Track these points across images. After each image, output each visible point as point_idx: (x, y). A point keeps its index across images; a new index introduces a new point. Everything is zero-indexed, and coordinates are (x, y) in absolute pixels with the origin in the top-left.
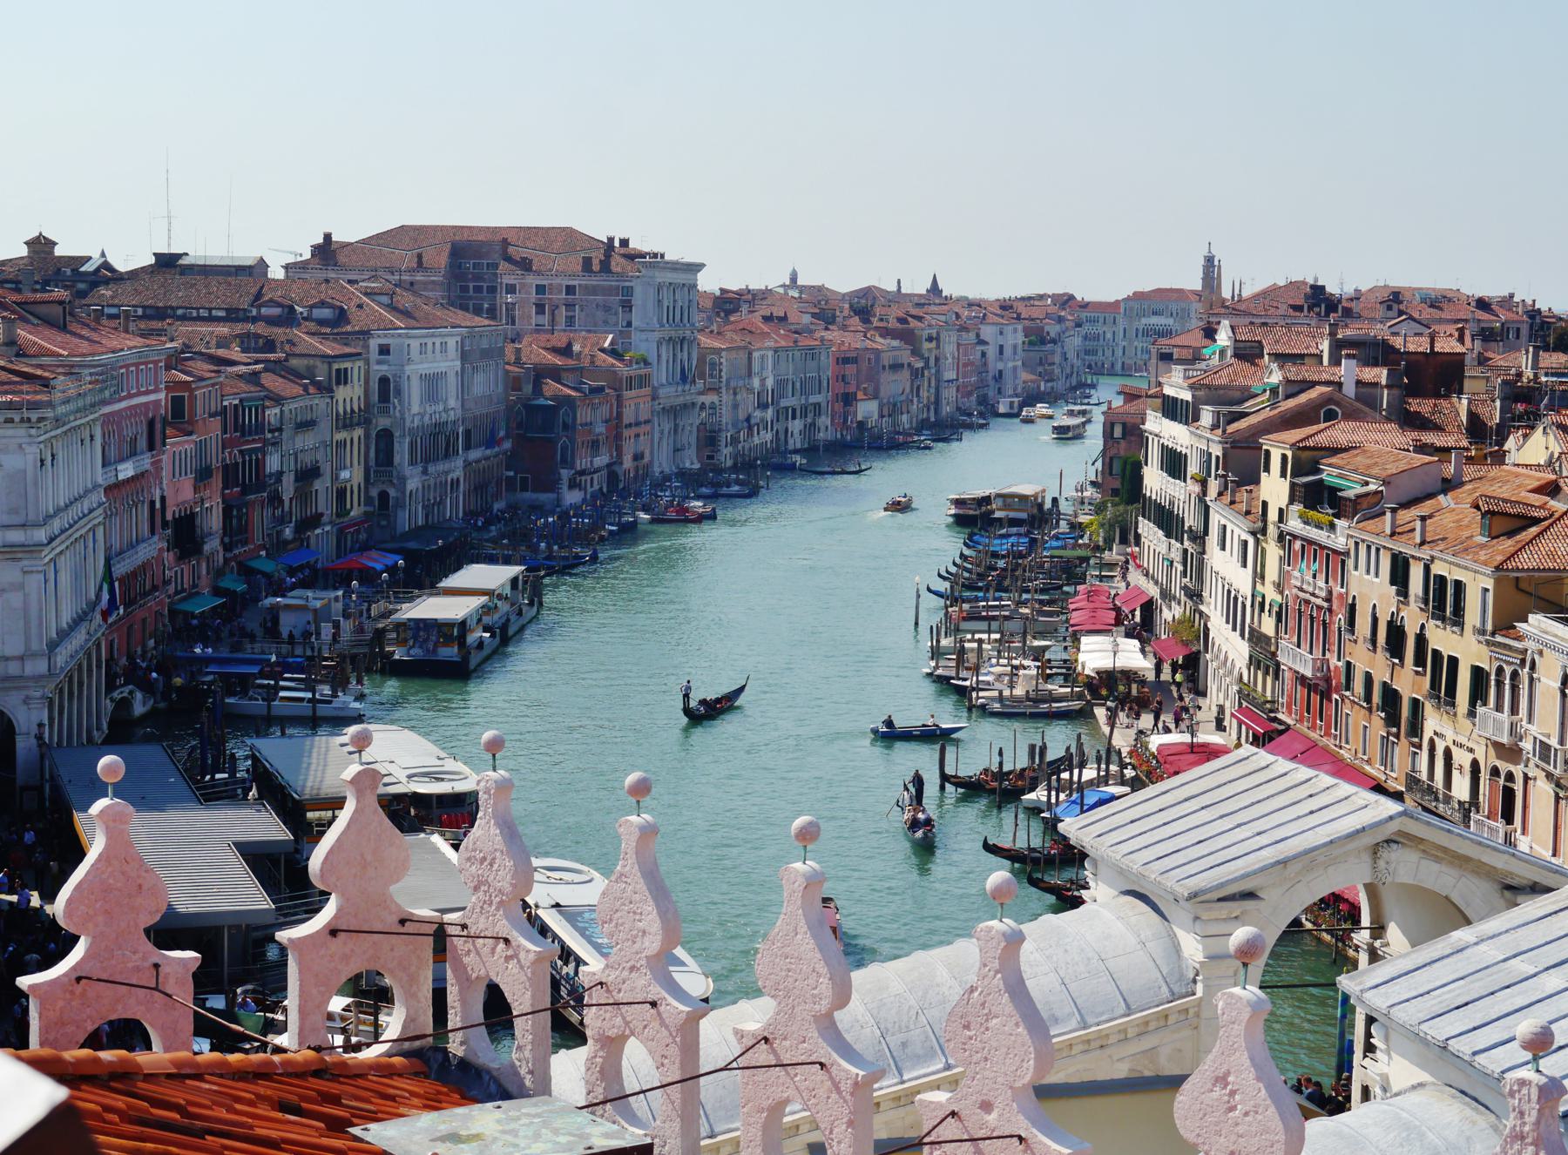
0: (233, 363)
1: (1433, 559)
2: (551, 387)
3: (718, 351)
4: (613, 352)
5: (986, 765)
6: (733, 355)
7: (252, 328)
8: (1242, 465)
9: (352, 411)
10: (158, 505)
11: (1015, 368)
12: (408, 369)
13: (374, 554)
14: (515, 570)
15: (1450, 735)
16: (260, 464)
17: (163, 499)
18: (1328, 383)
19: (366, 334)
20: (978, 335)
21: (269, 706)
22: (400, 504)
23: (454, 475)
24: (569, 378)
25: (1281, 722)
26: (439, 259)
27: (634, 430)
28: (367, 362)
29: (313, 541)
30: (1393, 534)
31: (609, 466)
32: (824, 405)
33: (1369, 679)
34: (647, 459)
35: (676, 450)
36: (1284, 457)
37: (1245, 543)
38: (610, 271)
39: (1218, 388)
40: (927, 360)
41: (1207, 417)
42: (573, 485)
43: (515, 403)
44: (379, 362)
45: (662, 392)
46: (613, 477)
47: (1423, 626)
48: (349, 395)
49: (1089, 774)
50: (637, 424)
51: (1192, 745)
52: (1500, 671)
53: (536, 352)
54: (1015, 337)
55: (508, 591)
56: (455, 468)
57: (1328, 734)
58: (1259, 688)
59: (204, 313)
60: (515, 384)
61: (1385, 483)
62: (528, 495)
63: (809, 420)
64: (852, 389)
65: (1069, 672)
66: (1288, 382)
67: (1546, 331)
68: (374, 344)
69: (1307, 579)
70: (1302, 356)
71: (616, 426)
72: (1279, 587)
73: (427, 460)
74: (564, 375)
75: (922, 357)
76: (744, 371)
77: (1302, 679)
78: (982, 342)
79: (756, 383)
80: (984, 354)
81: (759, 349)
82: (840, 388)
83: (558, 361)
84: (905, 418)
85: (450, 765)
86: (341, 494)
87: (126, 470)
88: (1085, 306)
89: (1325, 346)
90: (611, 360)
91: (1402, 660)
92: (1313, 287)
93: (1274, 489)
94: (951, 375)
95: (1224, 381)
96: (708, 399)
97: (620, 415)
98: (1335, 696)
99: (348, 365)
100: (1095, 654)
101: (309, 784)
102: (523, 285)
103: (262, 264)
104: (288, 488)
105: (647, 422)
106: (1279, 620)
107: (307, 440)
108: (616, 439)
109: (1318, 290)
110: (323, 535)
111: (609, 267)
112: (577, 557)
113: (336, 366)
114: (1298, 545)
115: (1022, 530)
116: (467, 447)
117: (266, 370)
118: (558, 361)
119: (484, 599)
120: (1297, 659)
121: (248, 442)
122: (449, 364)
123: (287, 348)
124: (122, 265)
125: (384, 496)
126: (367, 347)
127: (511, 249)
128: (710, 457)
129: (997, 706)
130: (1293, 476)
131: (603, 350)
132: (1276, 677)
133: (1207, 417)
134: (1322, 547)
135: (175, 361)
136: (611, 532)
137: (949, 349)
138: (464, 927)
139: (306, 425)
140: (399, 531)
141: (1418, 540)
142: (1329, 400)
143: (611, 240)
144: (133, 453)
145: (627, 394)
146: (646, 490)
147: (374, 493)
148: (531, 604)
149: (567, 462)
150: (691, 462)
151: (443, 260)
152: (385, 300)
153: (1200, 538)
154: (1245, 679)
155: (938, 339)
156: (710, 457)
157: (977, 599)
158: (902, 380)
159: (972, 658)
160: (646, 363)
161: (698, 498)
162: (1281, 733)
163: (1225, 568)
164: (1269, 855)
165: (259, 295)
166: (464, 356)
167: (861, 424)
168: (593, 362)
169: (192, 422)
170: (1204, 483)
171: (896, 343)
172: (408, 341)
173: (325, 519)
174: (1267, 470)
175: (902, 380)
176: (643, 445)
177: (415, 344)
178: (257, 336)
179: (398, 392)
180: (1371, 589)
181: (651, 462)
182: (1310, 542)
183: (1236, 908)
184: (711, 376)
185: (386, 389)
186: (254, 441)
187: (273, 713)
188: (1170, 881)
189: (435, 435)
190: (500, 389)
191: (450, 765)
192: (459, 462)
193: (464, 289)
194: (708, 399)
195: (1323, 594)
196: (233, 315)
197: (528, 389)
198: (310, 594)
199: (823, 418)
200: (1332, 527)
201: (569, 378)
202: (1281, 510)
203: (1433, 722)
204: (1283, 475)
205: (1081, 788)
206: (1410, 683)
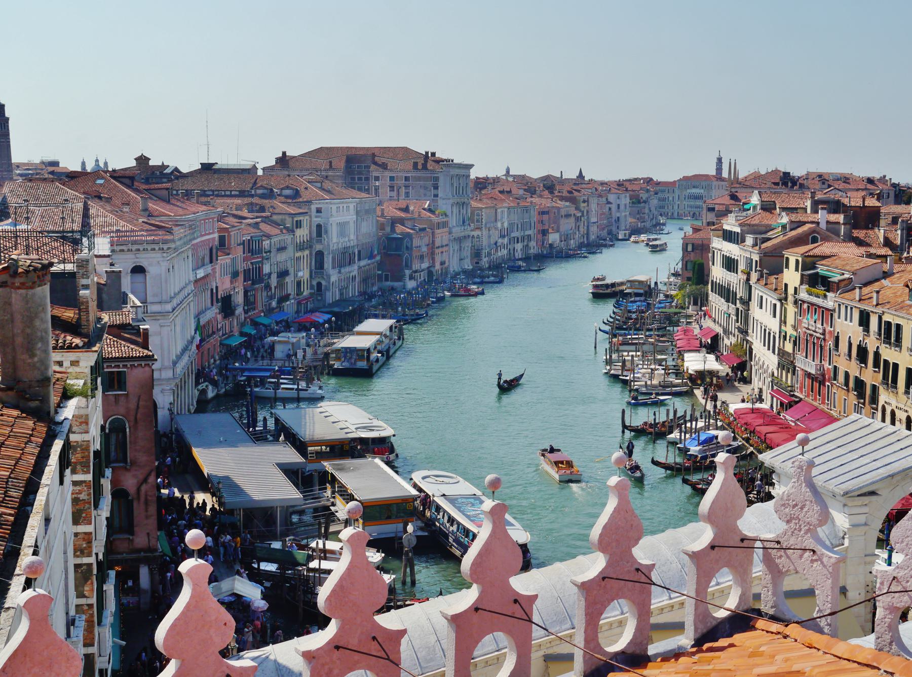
0: (245, 218)
1: (883, 313)
2: (400, 228)
4: (430, 210)
5: (646, 420)
6: (488, 211)
7: (250, 200)
8: (771, 265)
11: (625, 216)
13: (317, 314)
14: (391, 322)
15: (894, 403)
16: (260, 269)
17: (217, 287)
18: (812, 222)
19: (309, 202)
22: (327, 289)
23: (353, 274)
24: (409, 224)
25: (796, 397)
27: (440, 250)
28: (311, 217)
29: (285, 308)
30: (860, 300)
33: (847, 375)
34: (447, 264)
35: (461, 259)
36: (797, 261)
37: (775, 305)
39: (754, 225)
40: (583, 212)
41: (749, 240)
42: (411, 278)
44: (316, 217)
45: (454, 230)
46: (430, 273)
47: (878, 347)
48: (302, 234)
49: (701, 424)
50: (442, 246)
51: (753, 409)
53: (392, 211)
54: (625, 200)
55: (388, 333)
56: (354, 270)
57: (823, 403)
58: (784, 379)
59: (228, 193)
61: (854, 274)
62: (389, 283)
65: (678, 373)
66: (792, 222)
67: (902, 195)
69: (810, 322)
70: (796, 209)
71: (432, 247)
72: (795, 328)
73: (341, 266)
74: (406, 222)
76: (493, 219)
77: (809, 375)
78: (609, 203)
79: (499, 225)
80: (610, 209)
82: (540, 227)
83: (403, 215)
85: (376, 422)
87: (201, 273)
88: (658, 183)
89: (808, 204)
91: (866, 365)
92: (785, 173)
93: (791, 277)
94: (594, 220)
95: (757, 222)
96: (476, 233)
97: (433, 242)
98: (827, 383)
99: (301, 218)
100: (694, 362)
101: (307, 433)
102: (383, 177)
103: (255, 168)
104: (274, 281)
105: (447, 245)
106: (795, 343)
107: (282, 257)
108: (432, 254)
109: (786, 175)
110: (290, 306)
111: (427, 167)
112: (417, 314)
113: (295, 219)
114: (805, 306)
115: (642, 298)
116: (359, 259)
117: (262, 221)
118: (403, 215)
119: (378, 337)
120: (806, 364)
121: (254, 258)
123: (271, 210)
124: (185, 170)
125: (319, 284)
127: (376, 159)
128: (477, 263)
129: (644, 390)
130: (802, 270)
131: (424, 209)
132: (794, 373)
133: (749, 240)
134: (820, 307)
135: (221, 218)
136: (433, 302)
137: (594, 206)
138: (778, 542)
139: (282, 249)
140: (327, 302)
141: (875, 303)
142: (814, 231)
143: (427, 153)
144: (203, 265)
145: (437, 231)
146: (448, 280)
147: (314, 283)
148: (399, 339)
149: (408, 266)
150: (468, 265)
151: (342, 164)
152: (319, 185)
153: (746, 302)
154: (776, 374)
155: (588, 201)
156: (477, 263)
157: (626, 335)
159: (628, 365)
161: (474, 283)
162: (797, 402)
163: (763, 317)
164: (884, 472)
165: (255, 183)
166: (358, 213)
167: (551, 245)
169: (229, 248)
170: (748, 274)
171: (567, 204)
173: (291, 297)
174: (787, 267)
176: (445, 257)
177: (334, 207)
178: (257, 204)
179: (326, 232)
180: (848, 329)
182: (813, 304)
183: (866, 500)
184: (478, 221)
185: (320, 230)
187: (278, 396)
188: (831, 486)
189: (344, 253)
191: (376, 422)
192: (356, 267)
193: (353, 179)
194: (476, 233)
195: (821, 331)
196: (242, 194)
197: (388, 229)
198: (290, 335)
200: (825, 296)
201: (409, 224)
202: (796, 288)
203: (884, 396)
204: (797, 270)
205: (697, 431)
206: (871, 377)
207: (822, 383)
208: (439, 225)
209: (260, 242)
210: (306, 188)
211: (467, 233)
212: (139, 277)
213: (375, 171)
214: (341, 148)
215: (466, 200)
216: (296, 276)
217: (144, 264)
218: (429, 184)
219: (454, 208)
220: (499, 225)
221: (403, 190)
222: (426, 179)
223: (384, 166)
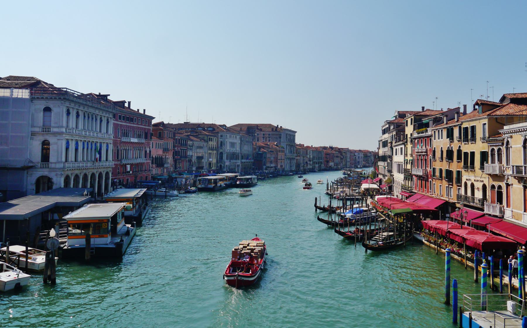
10: (148, 152)
17: (150, 151)
24: (267, 149)
26: (245, 129)
27: (280, 161)
28: (218, 138)
34: (283, 167)
42: (266, 169)
48: (213, 144)
52: (493, 150)
53: (260, 143)
54: (361, 155)
56: (239, 162)
60: (255, 149)
68: (219, 135)
72: (412, 155)
86: (210, 164)
96: (298, 158)
97: (277, 157)
107: (201, 151)
116: (242, 158)
122: (237, 141)
125: (221, 166)
132: (412, 180)
139: (201, 147)
147: (219, 165)
149: (265, 165)
150: (294, 168)
160: (283, 148)
166: (241, 141)
176: (283, 164)
179: (224, 144)
197: (257, 150)
207: (427, 180)
208: (280, 151)
209: (186, 141)
212: (47, 113)
216: (208, 160)
217: (51, 106)
220: (308, 156)
221: (268, 139)
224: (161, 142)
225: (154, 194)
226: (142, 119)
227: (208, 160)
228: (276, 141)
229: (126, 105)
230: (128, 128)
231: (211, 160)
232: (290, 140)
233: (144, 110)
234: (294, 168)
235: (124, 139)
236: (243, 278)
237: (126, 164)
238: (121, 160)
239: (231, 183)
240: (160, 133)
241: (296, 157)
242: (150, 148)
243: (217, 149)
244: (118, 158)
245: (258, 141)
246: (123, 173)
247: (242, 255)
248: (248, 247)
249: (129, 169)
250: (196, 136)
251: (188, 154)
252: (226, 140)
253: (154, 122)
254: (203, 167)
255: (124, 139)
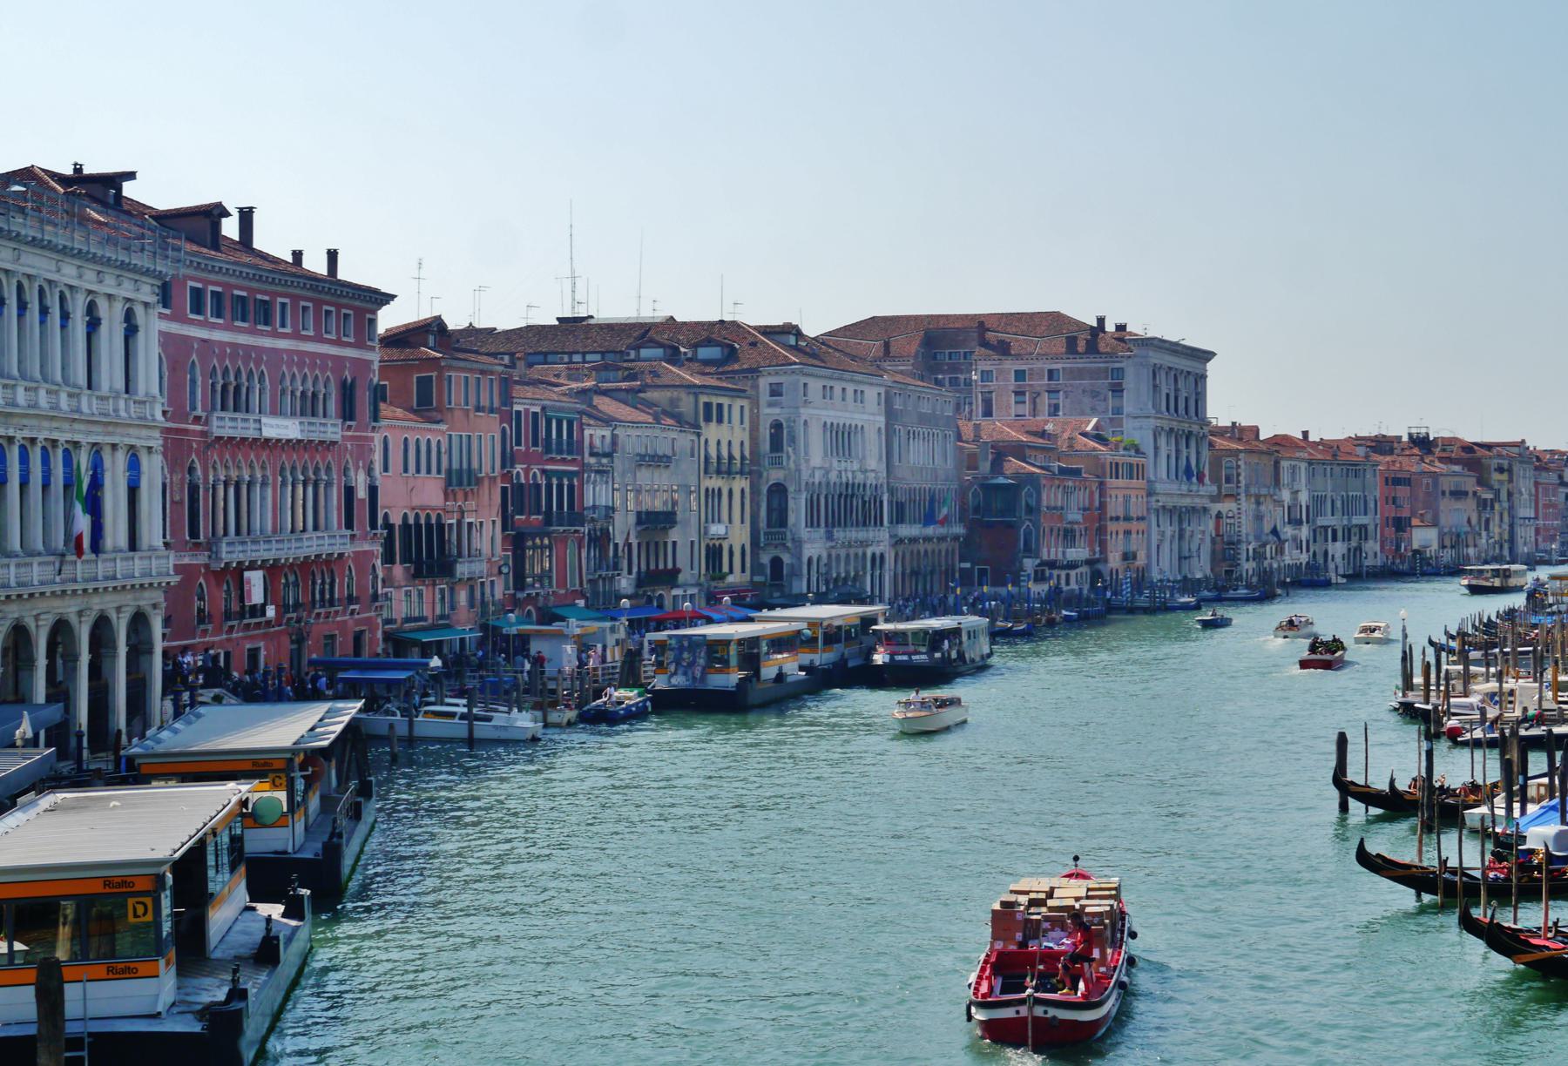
2: (1013, 464)
3: (1235, 453)
5: (1415, 774)
6: (1254, 459)
9: (731, 457)
10: (362, 493)
12: (805, 413)
17: (373, 491)
20: (1561, 477)
21: (411, 724)
22: (796, 573)
24: (1040, 459)
26: (909, 345)
27: (1122, 526)
28: (755, 403)
31: (1089, 562)
32: (1371, 528)
34: (1141, 561)
38: (1098, 352)
40: (1497, 493)
42: (1040, 577)
43: (971, 484)
44: (770, 405)
48: (727, 436)
50: (1127, 519)
56: (880, 540)
63: (1354, 544)
64: (1405, 514)
68: (764, 383)
74: (1028, 452)
75: (1491, 488)
81: (1291, 459)
84: (1471, 551)
86: (714, 554)
90: (1092, 444)
96: (1226, 507)
97: (1102, 506)
102: (1000, 372)
108: (1098, 532)
113: (703, 399)
121: (552, 461)
122: (867, 415)
125: (777, 563)
126: (756, 387)
127: (989, 335)
131: (1085, 434)
145: (1111, 482)
147: (765, 559)
149: (1030, 551)
155: (1510, 471)
158: (1468, 507)
160: (1138, 451)
166: (890, 414)
167: (1416, 552)
168: (1071, 446)
169: (439, 410)
171: (1457, 468)
172: (803, 380)
175: (1468, 507)
176: (1136, 543)
179: (793, 440)
181: (1148, 566)
184: (1228, 480)
186: (564, 461)
190: (950, 463)
197: (985, 466)
199: (1371, 543)
208: (1116, 470)
210: (754, 344)
211: (1198, 502)
213: (983, 363)
214: (916, 318)
215: (1195, 428)
216: (703, 532)
218: (1103, 384)
219: (1162, 441)
220: (1286, 496)
221: (1045, 401)
222: (1095, 374)
223: (1003, 349)
224: (434, 434)
225: (402, 730)
226: (318, 304)
227: (703, 532)
228: (1094, 411)
229: (230, 228)
230: (246, 359)
231: (717, 529)
232: (1172, 403)
233: (332, 256)
234: (1201, 568)
235: (225, 425)
236: (1053, 1012)
237: (240, 569)
238: (211, 546)
239: (843, 661)
240: (425, 384)
241: (1215, 499)
242: (370, 471)
243: (751, 468)
244: (194, 533)
245: (988, 413)
246: (228, 616)
247: (1033, 930)
248: (1050, 903)
249: (257, 596)
250: (631, 397)
251: (589, 502)
252: (805, 413)
253: (388, 319)
254: (676, 571)
255: (225, 425)
